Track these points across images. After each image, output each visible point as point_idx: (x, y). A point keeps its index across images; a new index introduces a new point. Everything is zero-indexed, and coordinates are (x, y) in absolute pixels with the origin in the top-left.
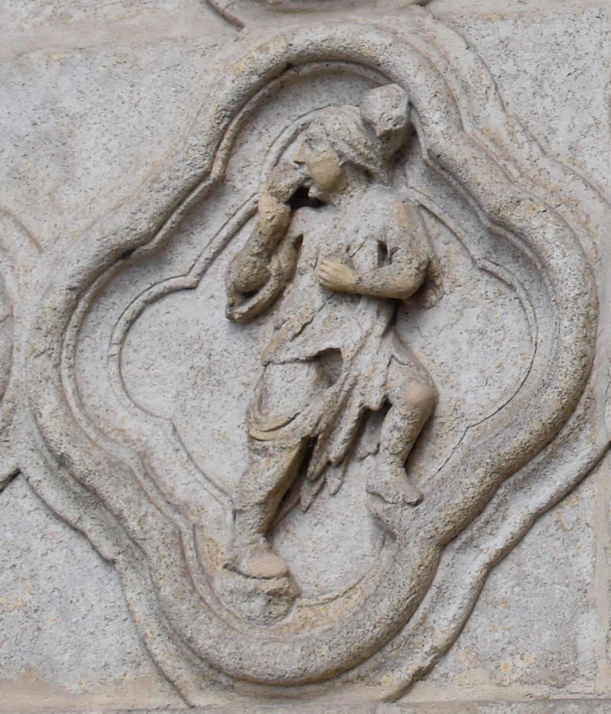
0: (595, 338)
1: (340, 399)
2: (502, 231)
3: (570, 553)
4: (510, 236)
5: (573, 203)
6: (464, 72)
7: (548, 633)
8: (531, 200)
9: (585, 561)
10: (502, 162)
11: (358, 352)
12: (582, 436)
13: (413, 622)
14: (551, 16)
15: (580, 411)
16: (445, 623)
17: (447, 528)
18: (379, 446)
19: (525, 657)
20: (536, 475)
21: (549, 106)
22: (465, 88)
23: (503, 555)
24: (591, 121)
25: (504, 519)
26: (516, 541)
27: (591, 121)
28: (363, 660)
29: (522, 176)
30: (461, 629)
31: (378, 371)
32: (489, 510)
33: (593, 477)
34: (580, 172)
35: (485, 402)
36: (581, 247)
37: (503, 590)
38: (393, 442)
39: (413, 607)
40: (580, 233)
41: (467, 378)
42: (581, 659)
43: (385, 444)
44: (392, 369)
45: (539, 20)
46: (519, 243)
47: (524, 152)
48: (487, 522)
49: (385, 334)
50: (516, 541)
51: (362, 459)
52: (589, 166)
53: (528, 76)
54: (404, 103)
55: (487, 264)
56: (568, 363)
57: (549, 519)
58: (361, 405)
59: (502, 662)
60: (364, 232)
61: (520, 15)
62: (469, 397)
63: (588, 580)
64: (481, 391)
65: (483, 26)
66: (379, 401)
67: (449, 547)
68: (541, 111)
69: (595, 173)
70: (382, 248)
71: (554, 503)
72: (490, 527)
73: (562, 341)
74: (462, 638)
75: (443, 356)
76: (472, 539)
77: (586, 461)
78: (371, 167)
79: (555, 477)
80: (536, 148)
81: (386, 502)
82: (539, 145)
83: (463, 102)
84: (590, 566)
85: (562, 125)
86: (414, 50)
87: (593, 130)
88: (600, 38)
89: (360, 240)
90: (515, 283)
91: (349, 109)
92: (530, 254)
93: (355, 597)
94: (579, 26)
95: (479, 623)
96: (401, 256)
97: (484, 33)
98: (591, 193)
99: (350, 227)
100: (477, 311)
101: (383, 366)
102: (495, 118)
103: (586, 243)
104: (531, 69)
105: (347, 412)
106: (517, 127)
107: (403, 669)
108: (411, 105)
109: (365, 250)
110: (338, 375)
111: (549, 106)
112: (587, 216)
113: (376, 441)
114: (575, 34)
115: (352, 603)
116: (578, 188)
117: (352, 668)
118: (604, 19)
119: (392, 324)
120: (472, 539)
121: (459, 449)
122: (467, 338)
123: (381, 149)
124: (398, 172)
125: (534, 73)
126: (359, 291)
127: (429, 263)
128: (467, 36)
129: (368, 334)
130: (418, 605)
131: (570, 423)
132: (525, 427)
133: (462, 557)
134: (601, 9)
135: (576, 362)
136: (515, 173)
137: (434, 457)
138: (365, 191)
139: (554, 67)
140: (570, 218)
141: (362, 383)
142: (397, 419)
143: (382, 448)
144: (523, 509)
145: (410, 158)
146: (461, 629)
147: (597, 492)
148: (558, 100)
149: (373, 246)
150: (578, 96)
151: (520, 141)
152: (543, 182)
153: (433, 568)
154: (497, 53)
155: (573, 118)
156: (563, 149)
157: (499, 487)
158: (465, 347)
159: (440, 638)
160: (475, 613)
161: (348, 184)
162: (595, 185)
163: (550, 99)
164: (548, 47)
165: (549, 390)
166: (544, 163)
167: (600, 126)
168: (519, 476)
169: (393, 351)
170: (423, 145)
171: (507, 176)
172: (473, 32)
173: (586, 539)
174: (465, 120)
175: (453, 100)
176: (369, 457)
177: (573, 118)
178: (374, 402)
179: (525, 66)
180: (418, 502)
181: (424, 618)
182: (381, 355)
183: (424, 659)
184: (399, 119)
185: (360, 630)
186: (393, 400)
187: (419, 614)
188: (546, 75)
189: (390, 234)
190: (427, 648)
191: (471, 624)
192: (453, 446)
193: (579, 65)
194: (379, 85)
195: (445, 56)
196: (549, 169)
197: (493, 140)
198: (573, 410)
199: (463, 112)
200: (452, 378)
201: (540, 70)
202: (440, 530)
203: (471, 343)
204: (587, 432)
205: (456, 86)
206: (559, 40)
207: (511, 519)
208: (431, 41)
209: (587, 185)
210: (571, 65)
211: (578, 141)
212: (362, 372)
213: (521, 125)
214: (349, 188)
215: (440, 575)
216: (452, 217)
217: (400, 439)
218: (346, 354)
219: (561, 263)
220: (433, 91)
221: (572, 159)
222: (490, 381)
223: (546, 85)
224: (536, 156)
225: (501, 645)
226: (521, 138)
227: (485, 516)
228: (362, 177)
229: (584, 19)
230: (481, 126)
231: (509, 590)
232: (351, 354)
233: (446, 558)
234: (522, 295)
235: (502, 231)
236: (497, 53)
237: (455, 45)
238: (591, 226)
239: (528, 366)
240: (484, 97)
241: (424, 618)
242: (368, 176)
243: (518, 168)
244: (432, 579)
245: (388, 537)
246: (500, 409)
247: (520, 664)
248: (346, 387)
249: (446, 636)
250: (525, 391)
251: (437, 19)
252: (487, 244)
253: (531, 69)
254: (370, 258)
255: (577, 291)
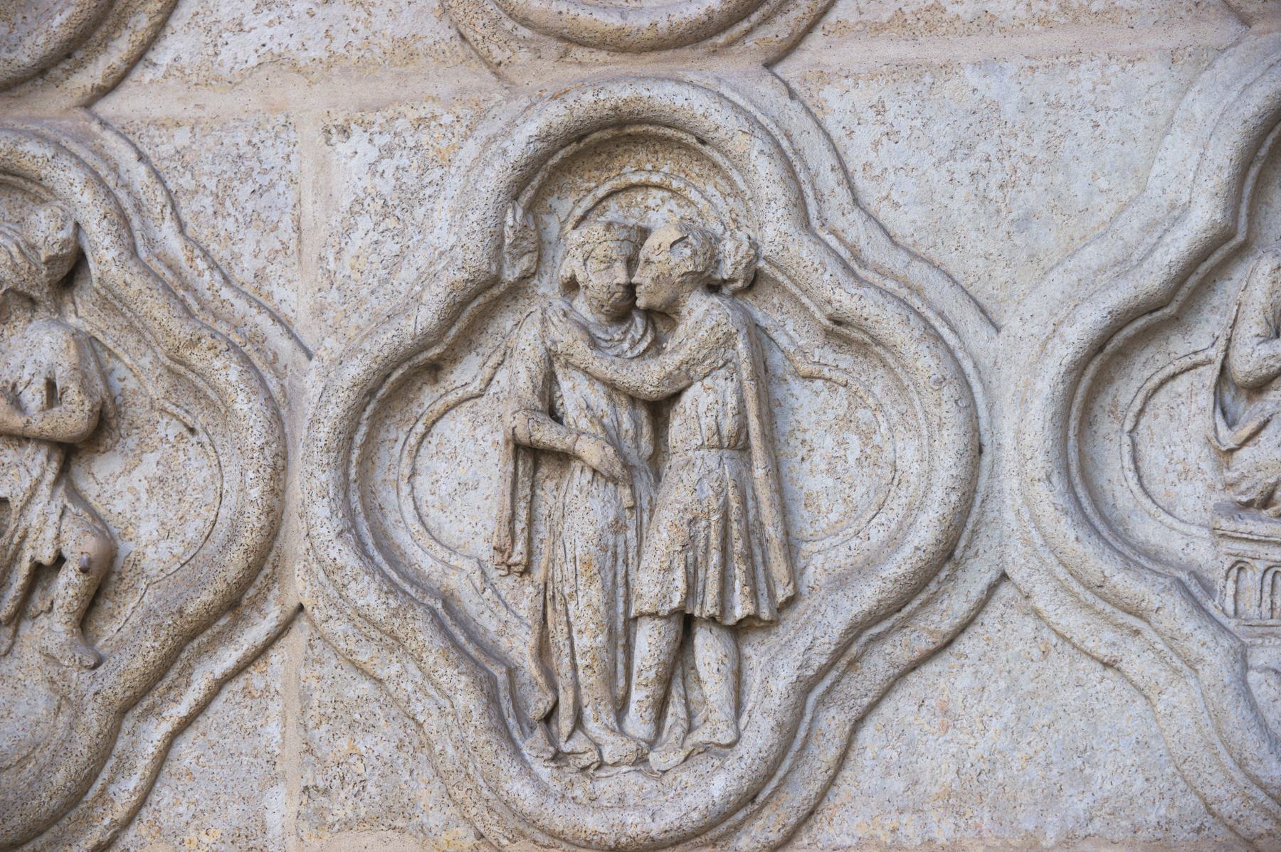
0: (284, 491)
1: (10, 552)
2: (182, 369)
3: (259, 723)
4: (191, 376)
5: (258, 340)
6: (137, 186)
7: (236, 806)
8: (213, 337)
9: (273, 729)
10: (181, 292)
11: (29, 501)
12: (270, 597)
13: (91, 794)
14: (232, 124)
15: (267, 570)
16: (126, 795)
17: (128, 694)
18: (52, 603)
19: (211, 832)
20: (223, 638)
21: (232, 227)
22: (138, 207)
23: (186, 723)
24: (278, 246)
25: (188, 685)
26: (201, 708)
27: (278, 246)
28: (40, 833)
29: (203, 309)
30: (142, 802)
31: (50, 523)
32: (172, 674)
33: (283, 641)
34: (268, 304)
35: (167, 557)
36: (267, 389)
37: (188, 761)
38: (68, 599)
39: (92, 777)
40: (268, 376)
41: (147, 530)
42: (270, 836)
43: (59, 602)
44: (66, 521)
45: (218, 128)
46: (200, 383)
47: (206, 280)
48: (170, 688)
49: (56, 483)
50: (201, 708)
51: (35, 617)
52: (277, 298)
53: (208, 192)
54: (70, 225)
55: (167, 405)
56: (254, 518)
57: (237, 685)
58: (32, 559)
59: (186, 838)
60: (29, 369)
61: (198, 121)
62: (150, 551)
63: (278, 751)
64: (163, 545)
65: (157, 133)
66: (52, 556)
67: (129, 715)
68: (223, 233)
69: (284, 304)
70: (51, 385)
71: (241, 669)
72: (173, 693)
73: (248, 494)
74: (144, 811)
75: (120, 505)
76: (154, 706)
77: (274, 623)
78: (36, 294)
79: (242, 640)
80: (218, 277)
81: (62, 665)
82: (222, 272)
83: (136, 223)
84: (279, 737)
85: (247, 248)
86: (81, 163)
87: (280, 257)
88: (287, 150)
89: (26, 378)
90: (198, 427)
91: (9, 228)
92: (213, 396)
93: (29, 766)
94: (263, 135)
95: (164, 795)
96: (73, 393)
97: (157, 140)
98: (278, 329)
99: (14, 362)
100: (156, 456)
101: (55, 518)
102: (174, 244)
103: (273, 385)
104: (212, 184)
105: (17, 567)
106: (197, 252)
107: (82, 843)
108: (77, 225)
109: (33, 387)
110: (7, 526)
111: (232, 227)
112: (275, 354)
113: (49, 599)
114: (259, 145)
115: (25, 773)
116: (265, 322)
117: (27, 841)
118: (291, 128)
119: (64, 471)
120: (154, 706)
121: (139, 609)
122: (147, 486)
123: (47, 276)
124: (67, 298)
125: (214, 189)
126: (27, 434)
127: (104, 403)
128: (139, 145)
129: (38, 482)
130: (97, 776)
131: (257, 582)
132: (208, 586)
133: (144, 726)
134: (287, 117)
135: (263, 517)
136: (195, 307)
137: (112, 616)
138: (30, 321)
139: (236, 183)
140: (255, 358)
141: (32, 536)
142: (72, 575)
143: (55, 607)
144: (208, 675)
145: (79, 284)
146: (142, 802)
147: (286, 658)
148: (241, 220)
149: (40, 383)
150: (263, 216)
151: (200, 268)
152: (227, 316)
153: (112, 736)
154: (173, 165)
155: (258, 242)
156: (248, 276)
157: (181, 650)
158: (144, 496)
159: (120, 811)
160: (158, 785)
161: (11, 313)
162: (283, 319)
163: (232, 220)
164: (230, 158)
165: (234, 548)
166: (226, 293)
167: (289, 252)
168: (203, 639)
169: (66, 501)
170: (93, 271)
171: (187, 309)
172: (146, 140)
173: (275, 707)
174: (140, 243)
175: (125, 220)
176: (42, 616)
177: (258, 242)
178: (46, 556)
179: (204, 180)
180: (95, 667)
181: (104, 790)
182: (53, 504)
183: (103, 834)
184: (65, 243)
185: (35, 802)
186: (66, 554)
187: (97, 786)
188: (229, 192)
189: (59, 371)
190: (107, 822)
191: (154, 798)
192: (132, 605)
193: (264, 181)
194: (43, 201)
195: (115, 169)
196: (233, 301)
197: (169, 267)
198: (261, 568)
199: (138, 234)
200: (130, 529)
201: (221, 186)
202: (120, 696)
203: (150, 491)
204: (276, 592)
205: (127, 203)
206: (241, 152)
207: (195, 686)
208: (99, 152)
209: (276, 318)
210: (254, 182)
211: (264, 268)
212: (33, 524)
213: (201, 249)
214: (13, 318)
215: (120, 745)
216: (127, 352)
217: (76, 597)
218: (16, 504)
219: (246, 408)
220: (102, 211)
221: (258, 289)
222: (172, 534)
223: (228, 203)
224: (217, 286)
225: (185, 818)
226: (201, 264)
227: (167, 681)
228: (27, 305)
229: (269, 127)
230: (157, 251)
231: (194, 761)
232: (19, 504)
233: (127, 725)
234: (205, 439)
235: (182, 369)
236: (173, 165)
237: (126, 156)
238: (279, 366)
239: (212, 518)
240: (160, 217)
241: (104, 790)
242: (33, 302)
243: (197, 299)
244: (112, 749)
245: (64, 702)
246: (183, 565)
247: (206, 839)
248: (16, 540)
249: (127, 809)
250: (210, 546)
251: (104, 124)
252: (166, 383)
253: (212, 184)
254: (38, 396)
255: (263, 440)
